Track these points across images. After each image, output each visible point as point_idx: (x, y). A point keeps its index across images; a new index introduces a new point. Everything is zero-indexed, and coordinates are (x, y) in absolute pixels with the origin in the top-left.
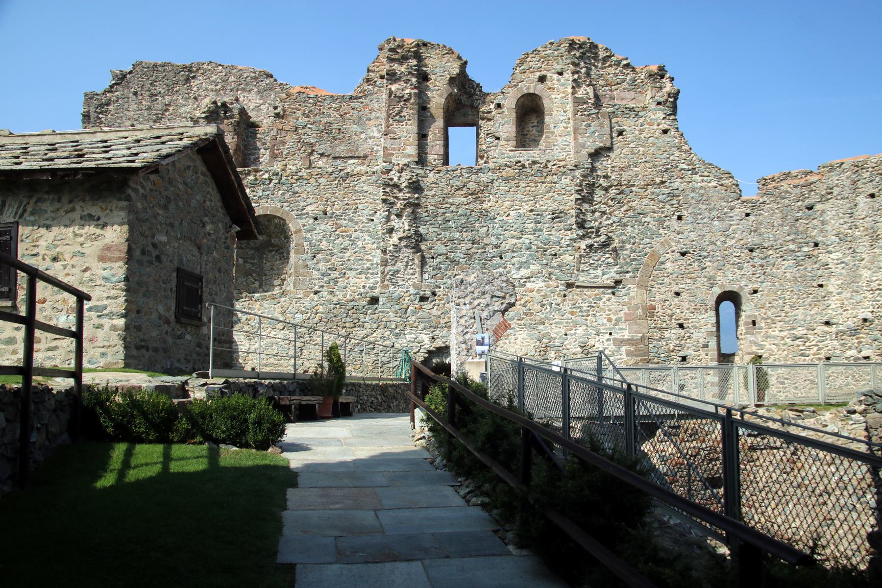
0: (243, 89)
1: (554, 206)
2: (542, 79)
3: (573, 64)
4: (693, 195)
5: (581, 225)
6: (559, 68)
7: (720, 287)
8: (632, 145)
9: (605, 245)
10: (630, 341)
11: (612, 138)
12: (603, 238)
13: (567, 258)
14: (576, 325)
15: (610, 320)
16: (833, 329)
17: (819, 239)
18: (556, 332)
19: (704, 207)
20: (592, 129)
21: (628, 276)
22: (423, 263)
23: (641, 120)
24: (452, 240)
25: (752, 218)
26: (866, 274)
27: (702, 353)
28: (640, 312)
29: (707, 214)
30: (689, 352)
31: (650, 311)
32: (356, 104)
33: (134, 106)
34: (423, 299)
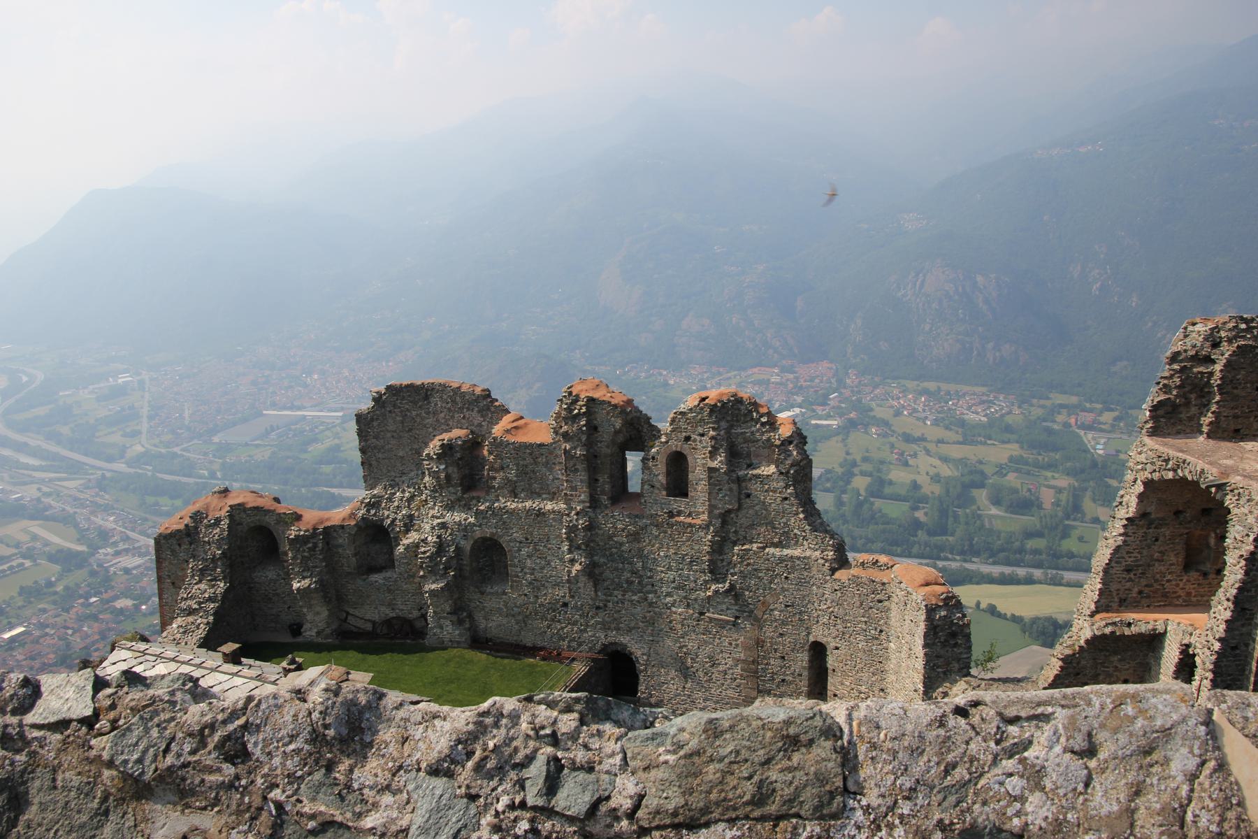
0: (468, 409)
2: (688, 439)
3: (714, 429)
5: (711, 572)
6: (700, 430)
8: (757, 508)
9: (728, 591)
10: (744, 661)
11: (739, 499)
12: (727, 585)
22: (595, 585)
24: (616, 569)
25: (839, 594)
31: (759, 643)
32: (543, 451)
33: (390, 421)
34: (598, 608)
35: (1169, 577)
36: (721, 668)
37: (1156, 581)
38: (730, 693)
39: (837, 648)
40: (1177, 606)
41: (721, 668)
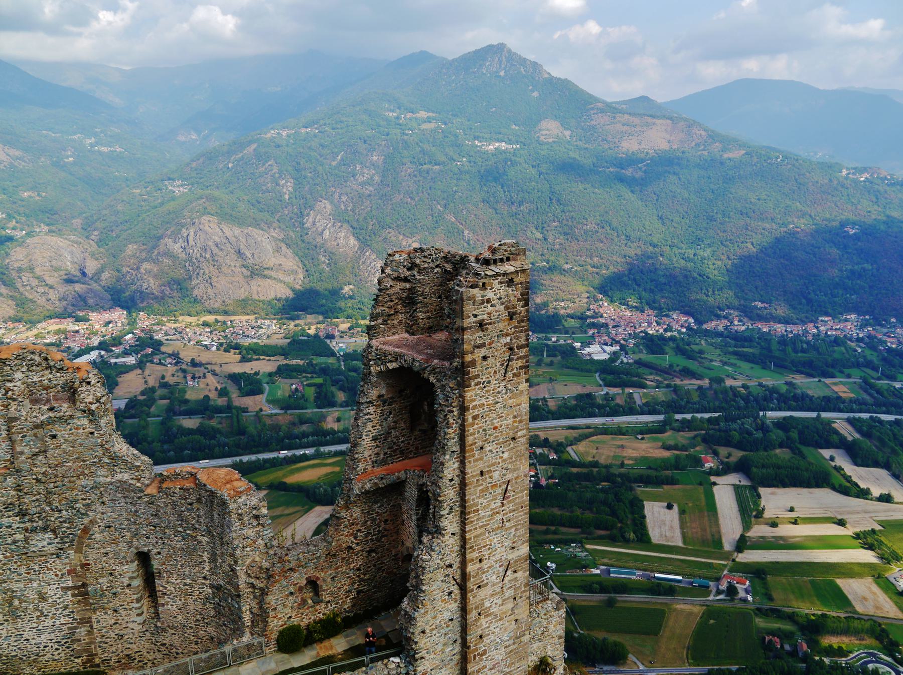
1: (4, 499)
4: (111, 487)
7: (136, 548)
10: (74, 588)
13: (19, 537)
14: (31, 580)
15: (57, 575)
16: (208, 582)
17: (197, 526)
18: (16, 586)
19: (120, 495)
20: (27, 439)
21: (67, 545)
23: (69, 426)
26: (220, 561)
27: (127, 591)
28: (78, 568)
29: (123, 500)
30: (119, 590)
35: (402, 439)
36: (50, 600)
37: (395, 443)
38: (62, 620)
39: (160, 553)
40: (410, 458)
41: (50, 600)
